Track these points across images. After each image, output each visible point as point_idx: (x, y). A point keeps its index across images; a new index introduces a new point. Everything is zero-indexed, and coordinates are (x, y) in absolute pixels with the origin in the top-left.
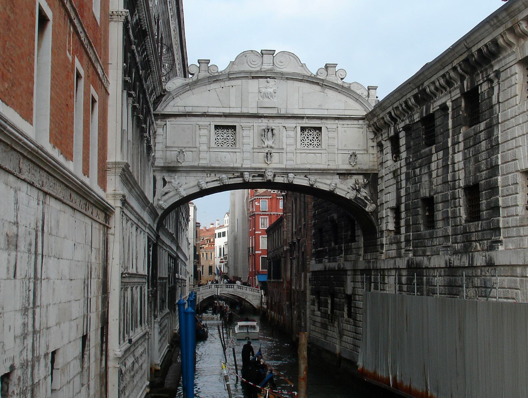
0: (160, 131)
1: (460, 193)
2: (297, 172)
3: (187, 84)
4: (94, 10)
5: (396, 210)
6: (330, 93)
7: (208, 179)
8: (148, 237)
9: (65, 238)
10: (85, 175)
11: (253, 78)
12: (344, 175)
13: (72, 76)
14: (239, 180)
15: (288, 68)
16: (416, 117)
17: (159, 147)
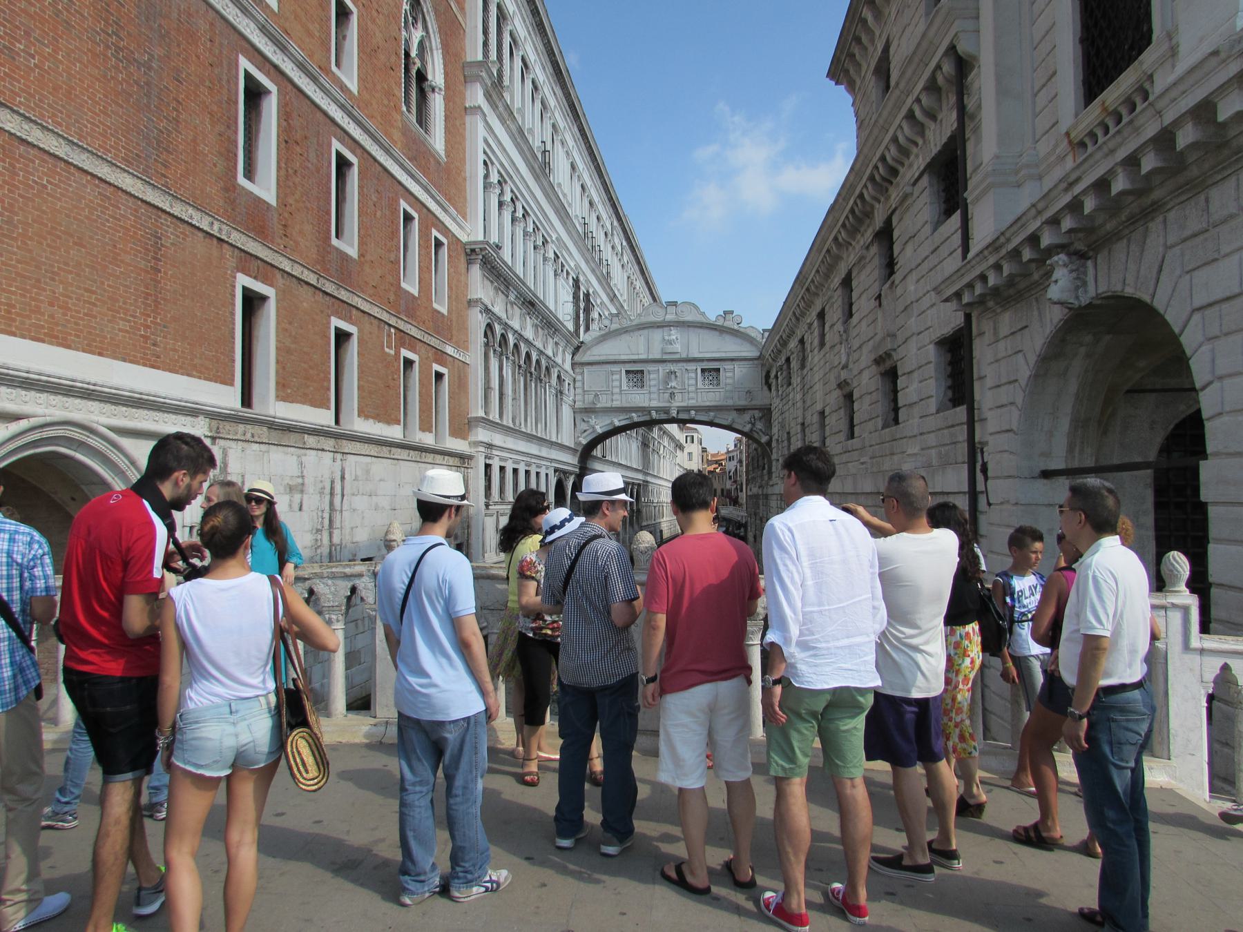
0: (579, 378)
1: (799, 427)
2: (698, 409)
3: (603, 336)
4: (435, 306)
5: (778, 440)
6: (728, 338)
7: (621, 418)
8: (556, 470)
9: (381, 480)
10: (424, 431)
11: (658, 327)
12: (741, 410)
13: (396, 364)
14: (647, 418)
15: (689, 318)
16: (783, 359)
17: (578, 391)
